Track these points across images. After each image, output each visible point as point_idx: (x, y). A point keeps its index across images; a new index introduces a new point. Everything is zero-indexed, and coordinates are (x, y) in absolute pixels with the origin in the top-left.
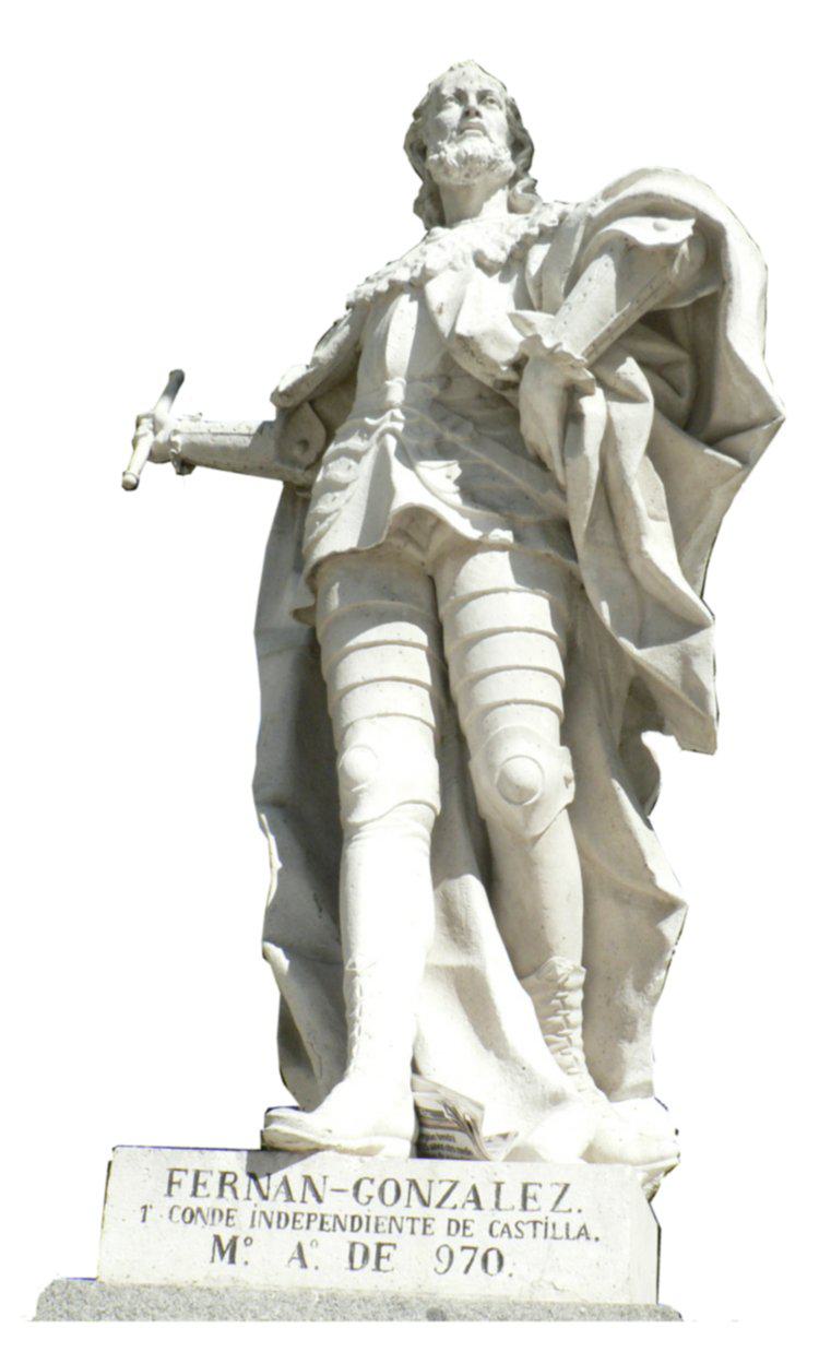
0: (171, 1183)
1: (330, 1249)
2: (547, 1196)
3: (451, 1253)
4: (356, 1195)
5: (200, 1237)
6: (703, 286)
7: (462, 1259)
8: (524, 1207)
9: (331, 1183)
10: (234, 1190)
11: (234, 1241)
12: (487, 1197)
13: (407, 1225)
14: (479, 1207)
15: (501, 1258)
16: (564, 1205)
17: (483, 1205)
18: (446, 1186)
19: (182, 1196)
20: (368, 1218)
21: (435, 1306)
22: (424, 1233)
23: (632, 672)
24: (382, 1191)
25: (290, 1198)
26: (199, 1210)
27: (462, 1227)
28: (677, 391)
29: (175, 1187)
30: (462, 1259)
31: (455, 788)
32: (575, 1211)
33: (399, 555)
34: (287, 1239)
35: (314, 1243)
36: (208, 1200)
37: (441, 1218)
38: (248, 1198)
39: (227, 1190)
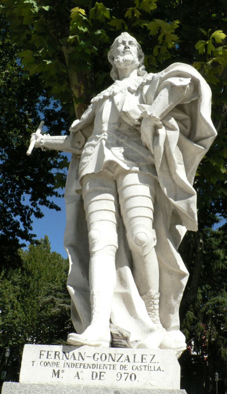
0: (41, 355)
1: (86, 374)
2: (148, 358)
3: (121, 375)
4: (94, 358)
5: (49, 370)
6: (194, 97)
7: (124, 376)
8: (142, 362)
10: (59, 357)
11: (59, 371)
12: (131, 359)
13: (108, 367)
14: (129, 361)
15: (135, 376)
16: (153, 361)
17: (130, 361)
18: (120, 355)
19: (44, 358)
20: (97, 364)
21: (116, 390)
22: (113, 369)
23: (173, 208)
24: (101, 357)
25: (75, 359)
26: (49, 362)
27: (124, 367)
28: (186, 128)
29: (42, 356)
30: (124, 376)
31: (122, 241)
32: (157, 363)
33: (106, 174)
34: (74, 371)
36: (51, 360)
37: (118, 365)
38: (63, 359)
39: (57, 356)
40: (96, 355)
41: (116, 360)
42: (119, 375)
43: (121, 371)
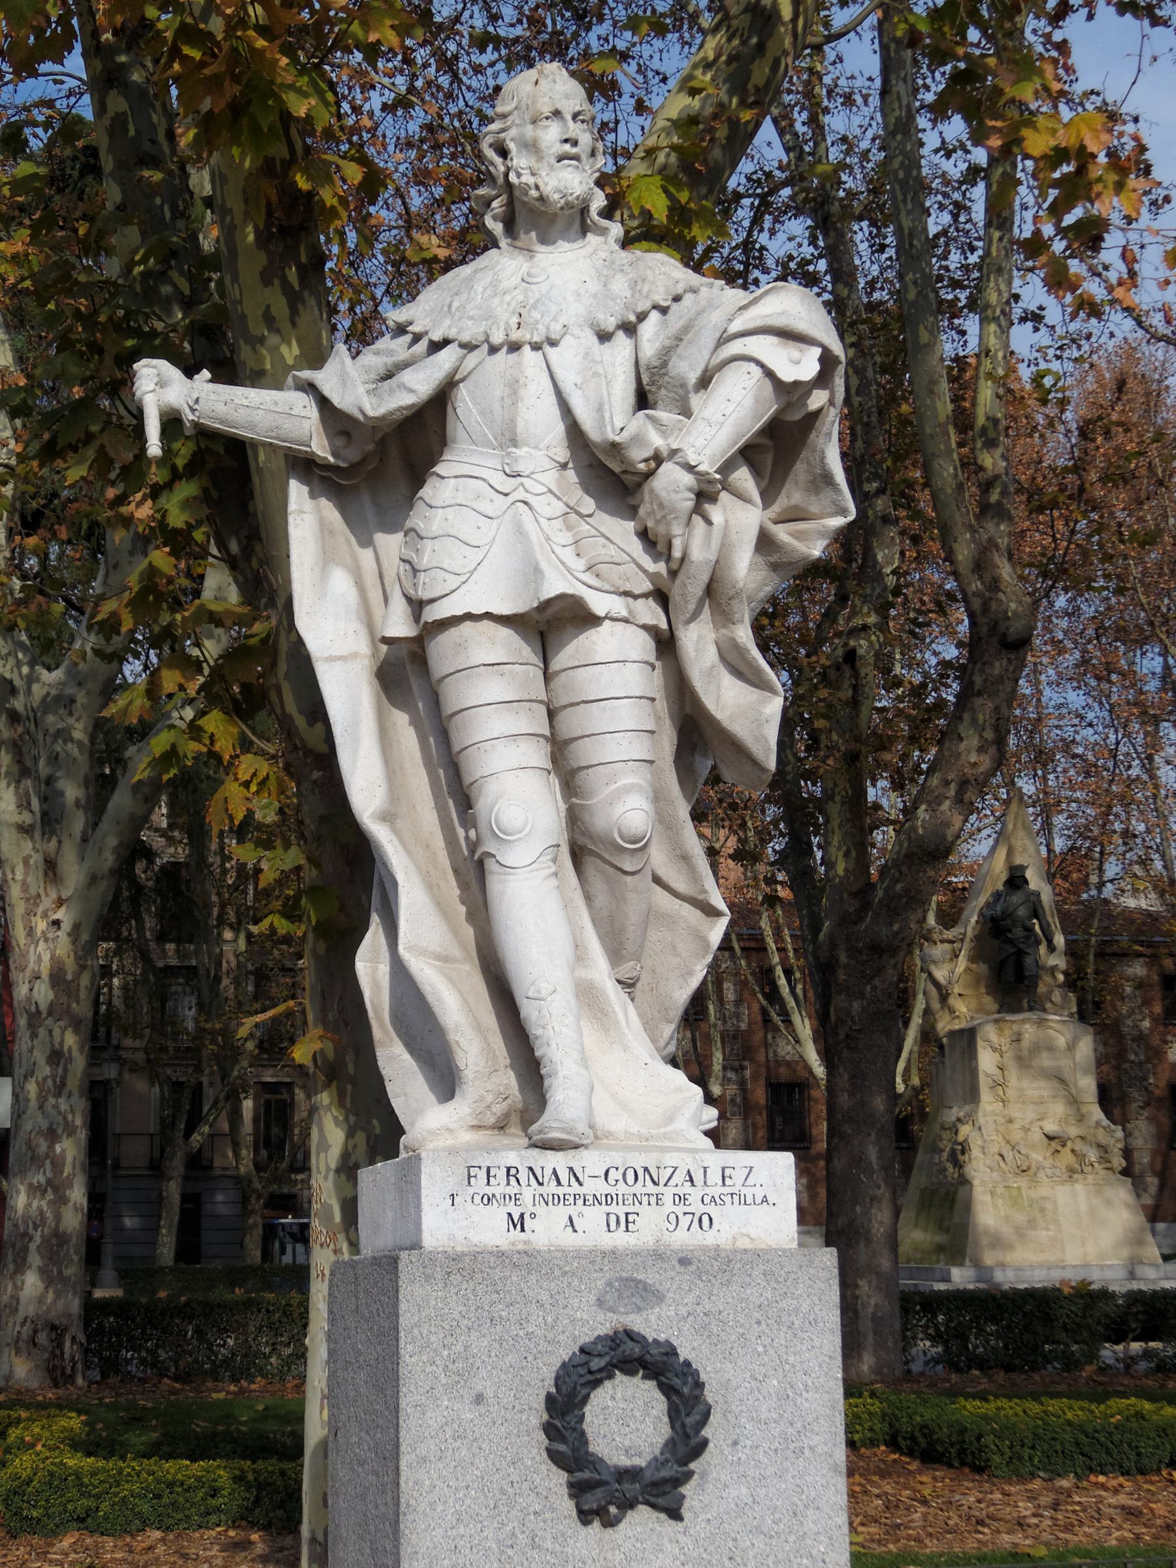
0: (469, 1177)
1: (592, 1219)
5: (497, 1215)
7: (685, 1221)
9: (588, 1172)
11: (522, 1216)
12: (698, 1177)
13: (645, 1200)
16: (750, 1181)
24: (624, 1174)
25: (559, 1183)
27: (682, 1199)
30: (685, 1221)
34: (560, 1213)
35: (581, 1215)
37: (668, 1193)
39: (512, 1179)
40: (612, 1172)
41: (662, 1182)
42: (673, 1218)
43: (676, 1209)
